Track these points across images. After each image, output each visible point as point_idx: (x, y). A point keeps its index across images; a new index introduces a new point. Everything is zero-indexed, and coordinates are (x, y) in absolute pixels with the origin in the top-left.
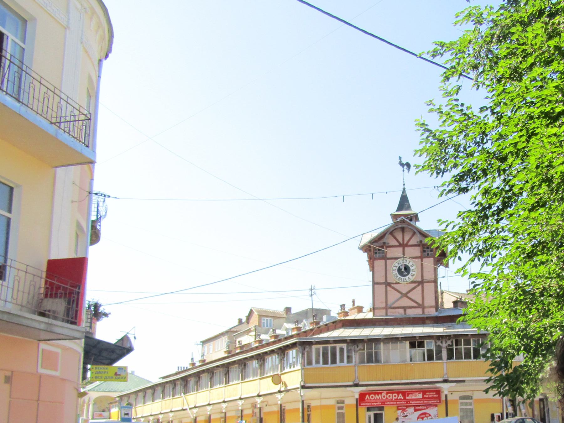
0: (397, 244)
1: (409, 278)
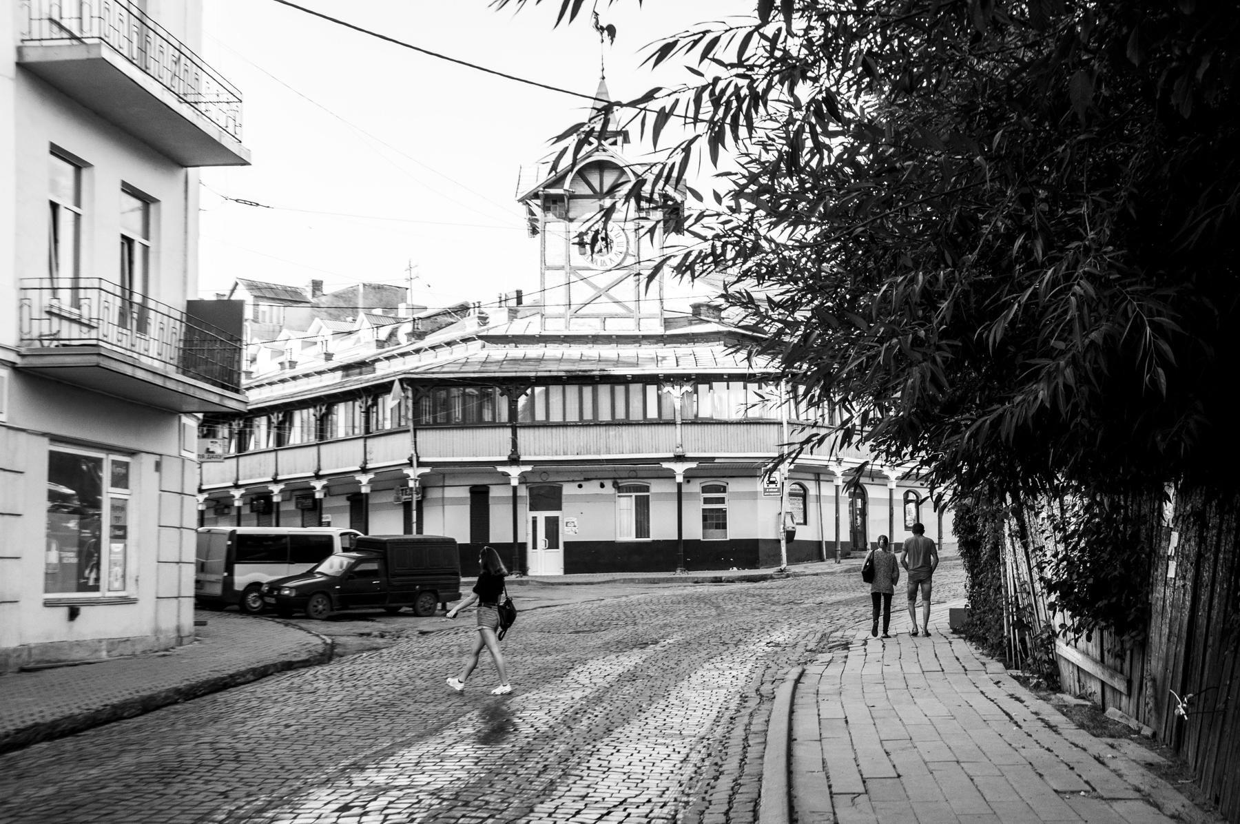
0: (590, 192)
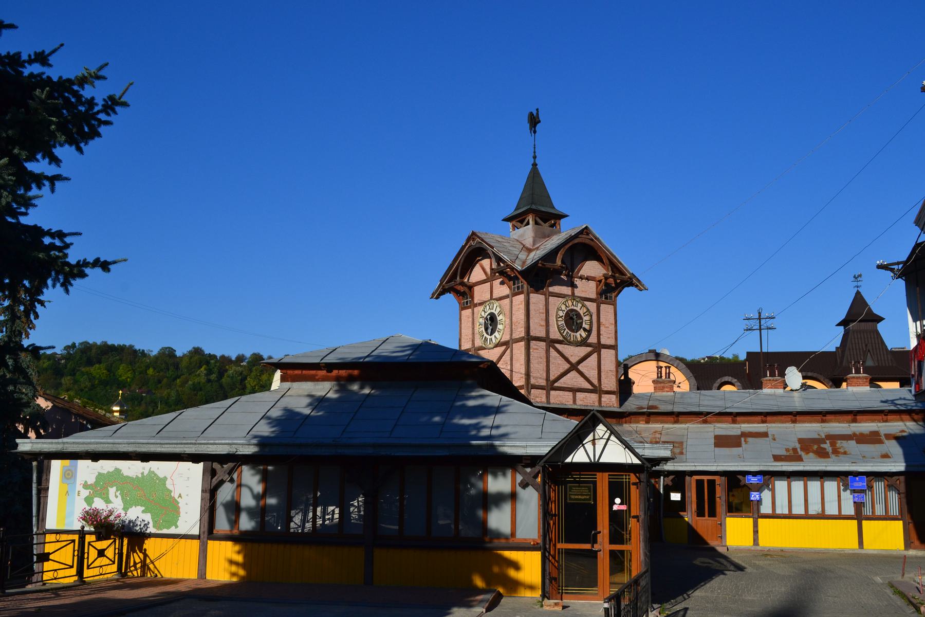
1: (495, 336)
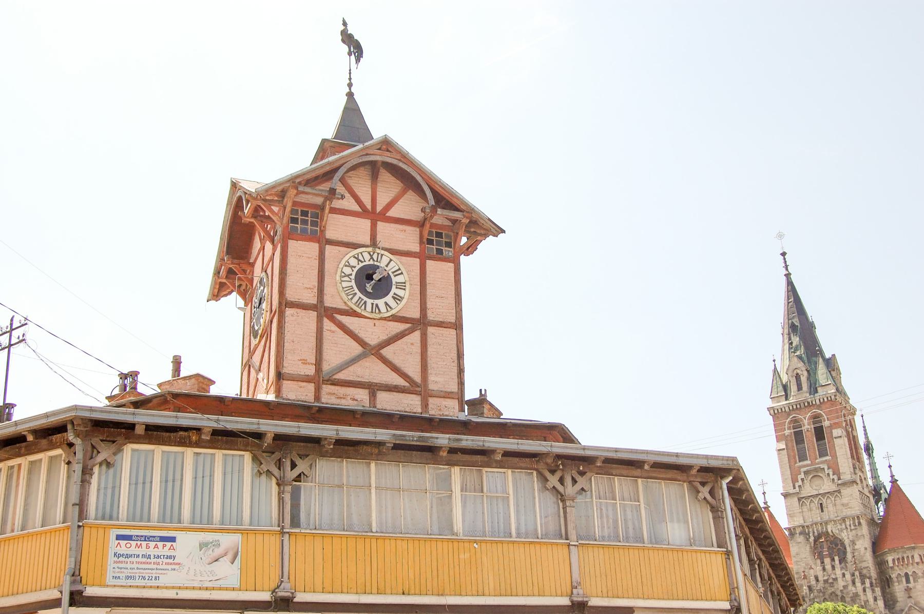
0: (356, 208)
1: (386, 304)
